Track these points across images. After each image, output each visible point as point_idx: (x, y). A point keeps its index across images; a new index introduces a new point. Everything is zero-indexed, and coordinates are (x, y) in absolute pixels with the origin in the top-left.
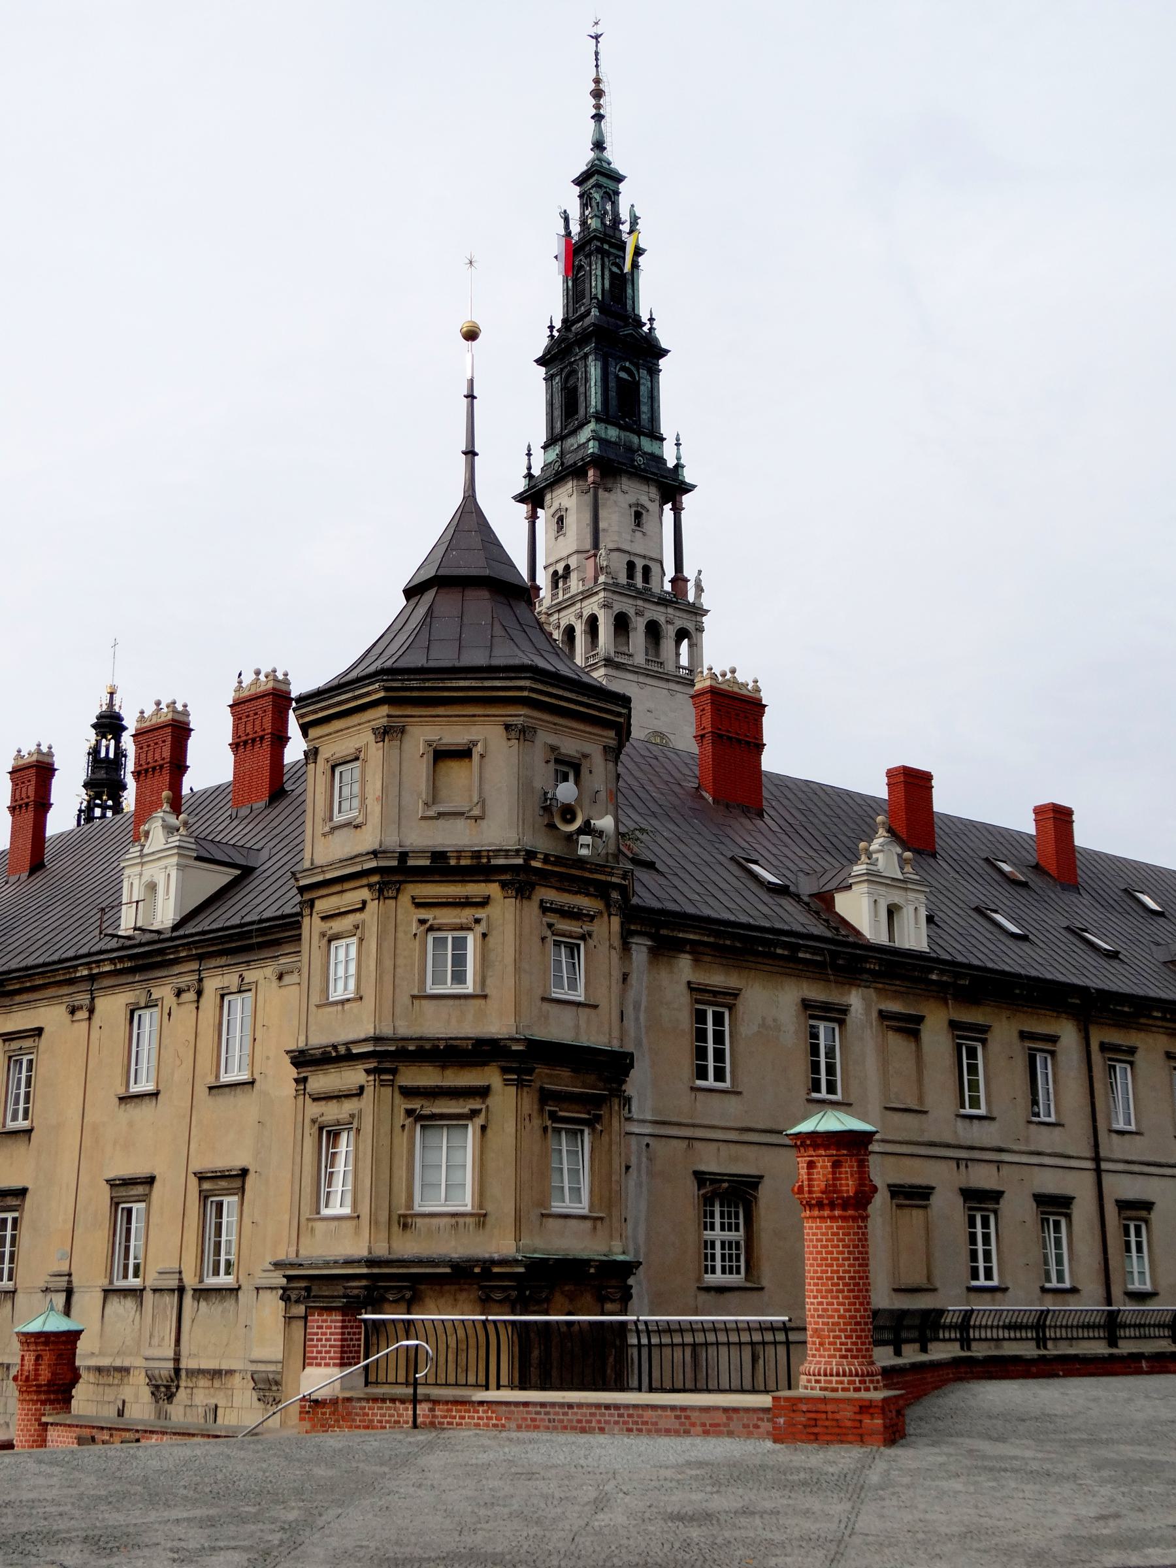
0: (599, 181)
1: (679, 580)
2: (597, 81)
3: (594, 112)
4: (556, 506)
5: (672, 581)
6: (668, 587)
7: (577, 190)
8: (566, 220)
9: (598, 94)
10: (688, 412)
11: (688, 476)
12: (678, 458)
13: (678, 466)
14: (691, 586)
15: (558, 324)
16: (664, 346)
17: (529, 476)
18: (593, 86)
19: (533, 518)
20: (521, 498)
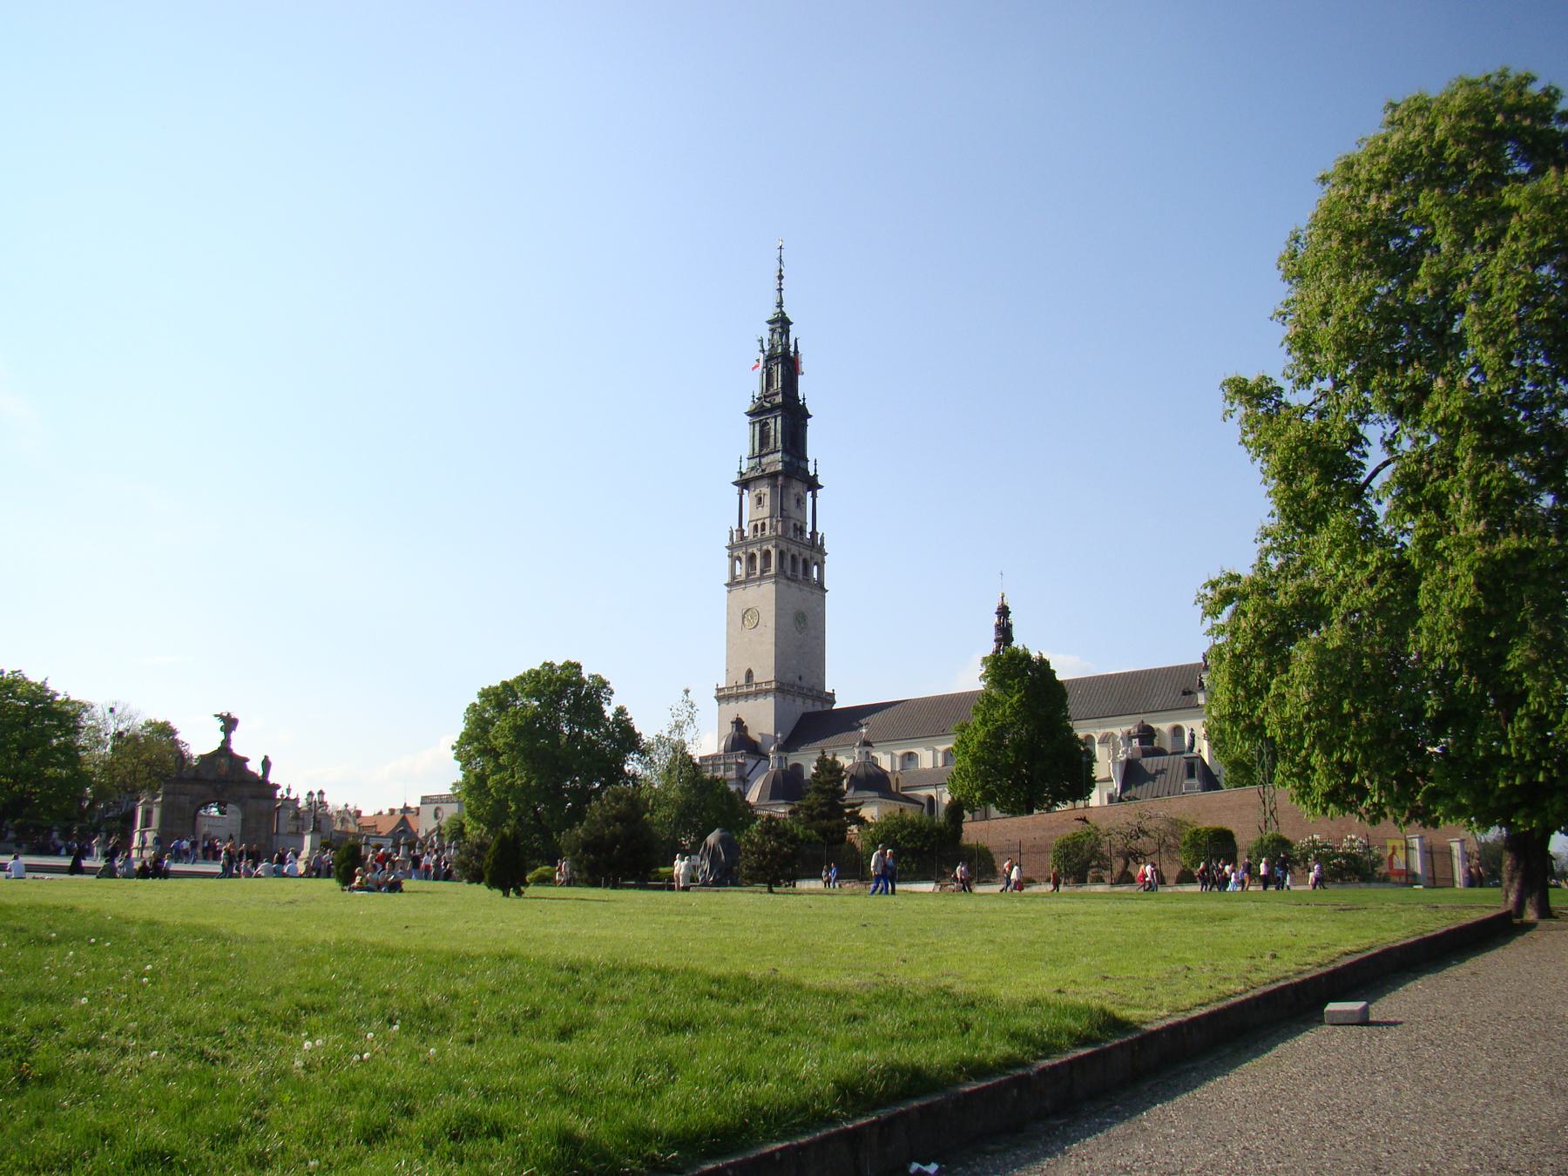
0: (781, 323)
1: (814, 533)
9: (781, 277)
10: (822, 448)
20: (735, 483)
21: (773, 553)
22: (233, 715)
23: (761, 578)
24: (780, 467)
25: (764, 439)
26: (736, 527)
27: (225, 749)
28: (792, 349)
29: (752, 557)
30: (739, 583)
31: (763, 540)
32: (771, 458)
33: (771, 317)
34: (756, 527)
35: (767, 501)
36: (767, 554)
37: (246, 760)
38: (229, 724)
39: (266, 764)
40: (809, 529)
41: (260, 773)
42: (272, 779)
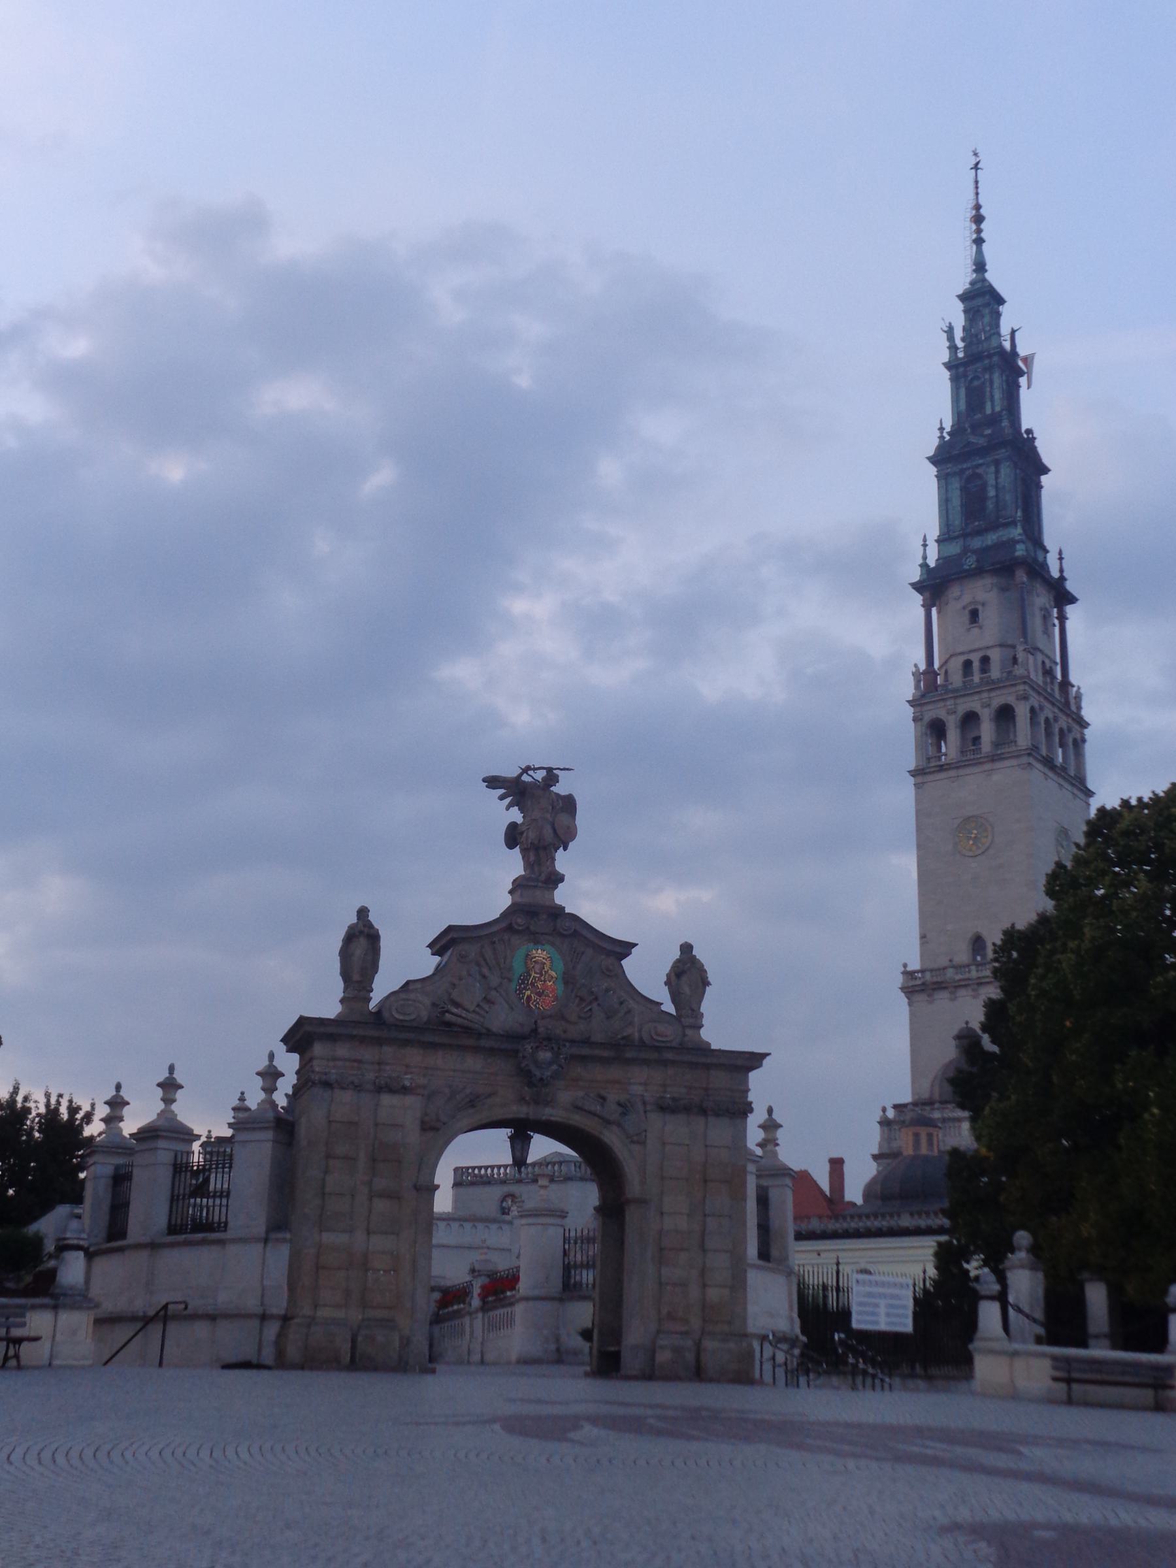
0: (982, 300)
1: (1066, 684)
3: (974, 236)
4: (967, 599)
8: (950, 332)
9: (978, 219)
12: (1061, 571)
13: (1062, 579)
14: (1075, 689)
15: (948, 429)
17: (924, 565)
20: (918, 587)
21: (1022, 712)
22: (560, 789)
23: (994, 758)
24: (1020, 551)
26: (922, 667)
27: (535, 913)
28: (1007, 345)
29: (970, 719)
30: (942, 768)
31: (994, 686)
32: (991, 538)
34: (968, 664)
35: (992, 618)
36: (1005, 714)
37: (625, 948)
38: (540, 814)
39: (688, 974)
41: (669, 1007)
42: (720, 1029)
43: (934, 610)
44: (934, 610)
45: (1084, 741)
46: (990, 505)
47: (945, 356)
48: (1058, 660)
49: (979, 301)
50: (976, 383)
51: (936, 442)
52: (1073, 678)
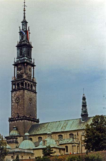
0: (25, 23)
1: (33, 78)
2: (24, 9)
3: (24, 13)
5: (33, 78)
6: (32, 79)
7: (21, 23)
8: (20, 27)
9: (24, 10)
11: (35, 64)
12: (34, 62)
13: (34, 63)
15: (19, 42)
16: (32, 46)
18: (24, 9)
19: (15, 68)
20: (13, 65)
24: (25, 61)
25: (21, 53)
26: (13, 76)
32: (23, 58)
33: (22, 20)
40: (32, 77)
43: (16, 67)
44: (16, 67)
45: (36, 86)
46: (23, 54)
47: (19, 31)
48: (32, 74)
49: (24, 23)
50: (23, 35)
51: (17, 44)
52: (34, 77)
